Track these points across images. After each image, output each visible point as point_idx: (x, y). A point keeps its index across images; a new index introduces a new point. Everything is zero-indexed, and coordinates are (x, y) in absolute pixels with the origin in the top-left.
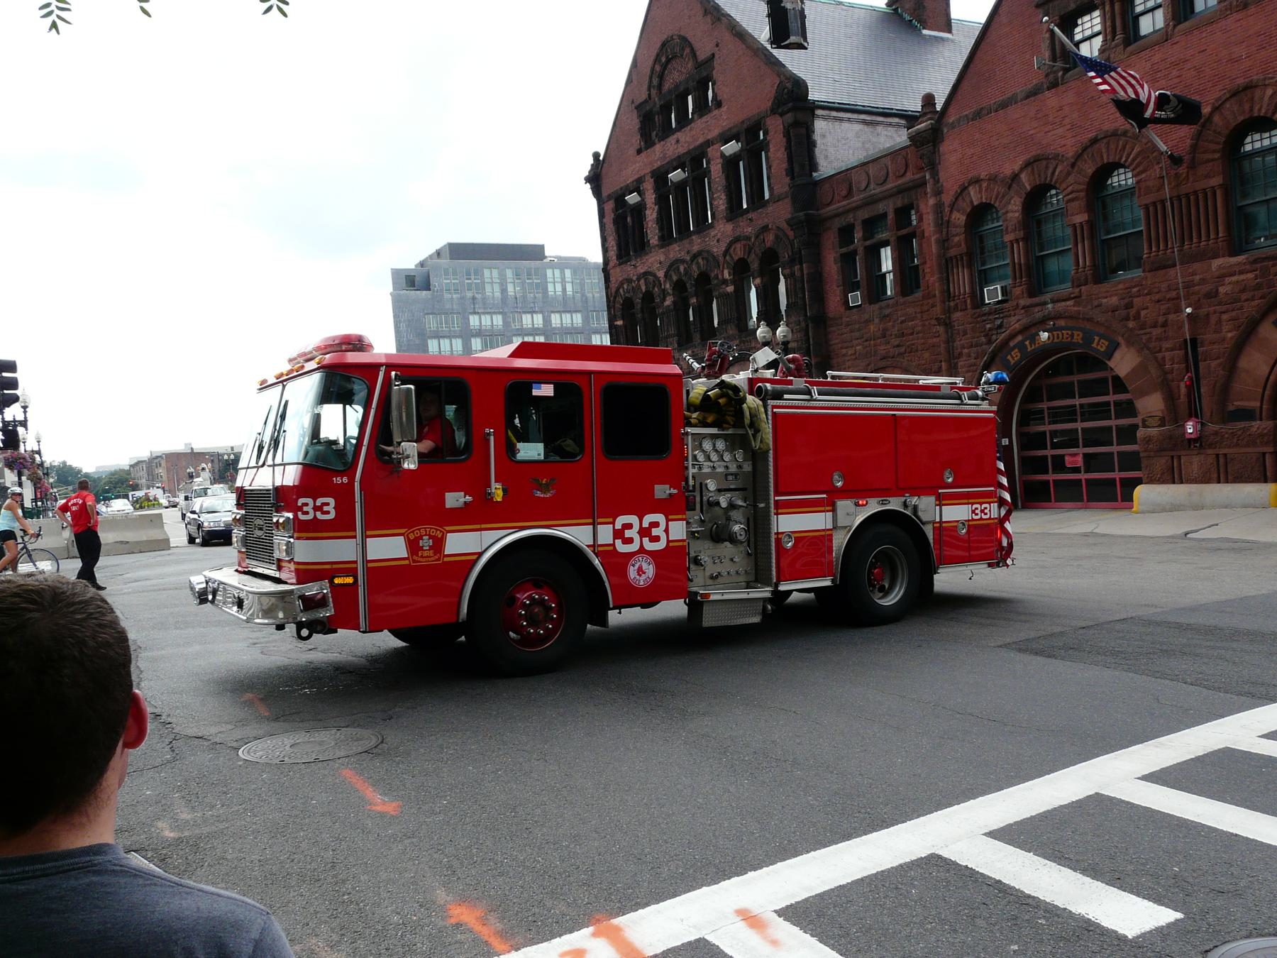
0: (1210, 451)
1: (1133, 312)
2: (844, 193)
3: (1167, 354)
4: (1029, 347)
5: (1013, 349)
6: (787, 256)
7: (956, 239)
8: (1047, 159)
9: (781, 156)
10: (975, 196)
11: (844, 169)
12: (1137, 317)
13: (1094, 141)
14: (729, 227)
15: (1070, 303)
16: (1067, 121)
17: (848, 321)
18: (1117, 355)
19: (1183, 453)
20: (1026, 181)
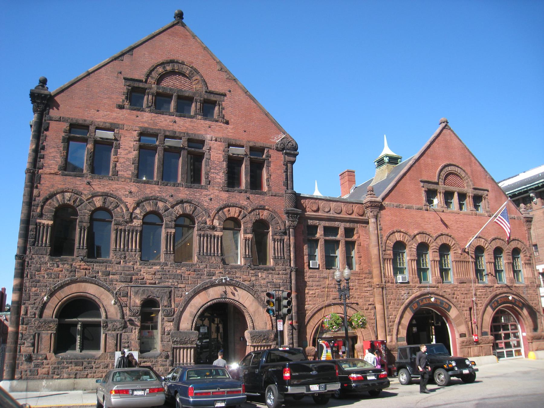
0: (478, 346)
1: (455, 296)
2: (315, 208)
3: (465, 312)
4: (421, 303)
5: (414, 303)
6: (279, 229)
7: (388, 252)
8: (426, 234)
9: (280, 173)
10: (398, 237)
11: (315, 197)
12: (456, 298)
13: (442, 235)
14: (225, 195)
15: (435, 288)
16: (431, 224)
17: (311, 275)
18: (451, 311)
19: (472, 346)
20: (419, 239)
